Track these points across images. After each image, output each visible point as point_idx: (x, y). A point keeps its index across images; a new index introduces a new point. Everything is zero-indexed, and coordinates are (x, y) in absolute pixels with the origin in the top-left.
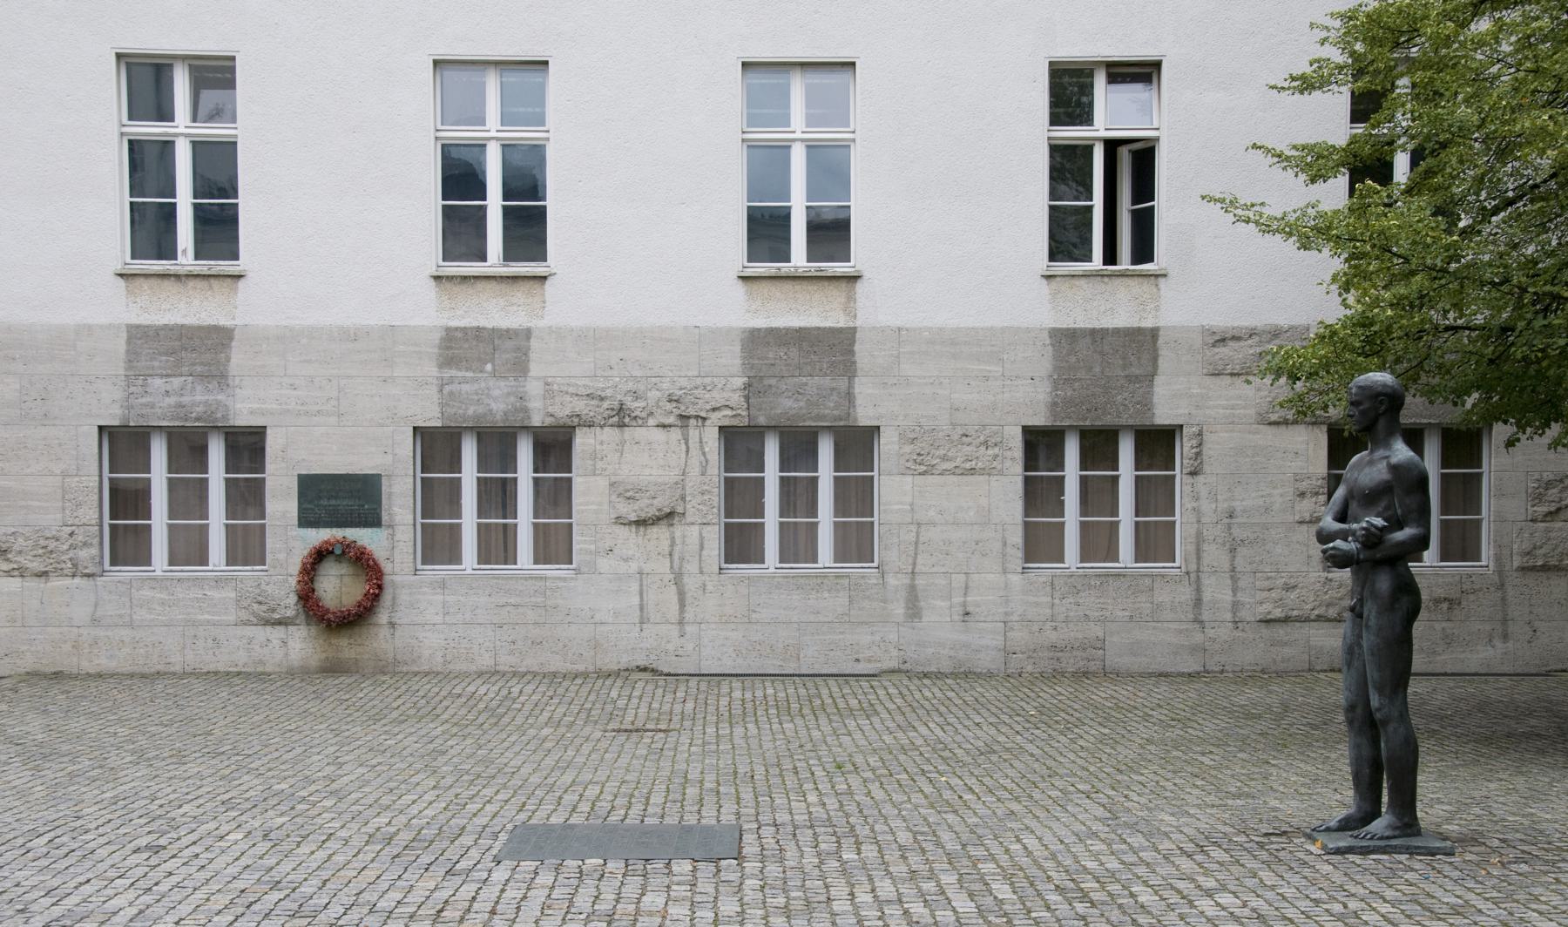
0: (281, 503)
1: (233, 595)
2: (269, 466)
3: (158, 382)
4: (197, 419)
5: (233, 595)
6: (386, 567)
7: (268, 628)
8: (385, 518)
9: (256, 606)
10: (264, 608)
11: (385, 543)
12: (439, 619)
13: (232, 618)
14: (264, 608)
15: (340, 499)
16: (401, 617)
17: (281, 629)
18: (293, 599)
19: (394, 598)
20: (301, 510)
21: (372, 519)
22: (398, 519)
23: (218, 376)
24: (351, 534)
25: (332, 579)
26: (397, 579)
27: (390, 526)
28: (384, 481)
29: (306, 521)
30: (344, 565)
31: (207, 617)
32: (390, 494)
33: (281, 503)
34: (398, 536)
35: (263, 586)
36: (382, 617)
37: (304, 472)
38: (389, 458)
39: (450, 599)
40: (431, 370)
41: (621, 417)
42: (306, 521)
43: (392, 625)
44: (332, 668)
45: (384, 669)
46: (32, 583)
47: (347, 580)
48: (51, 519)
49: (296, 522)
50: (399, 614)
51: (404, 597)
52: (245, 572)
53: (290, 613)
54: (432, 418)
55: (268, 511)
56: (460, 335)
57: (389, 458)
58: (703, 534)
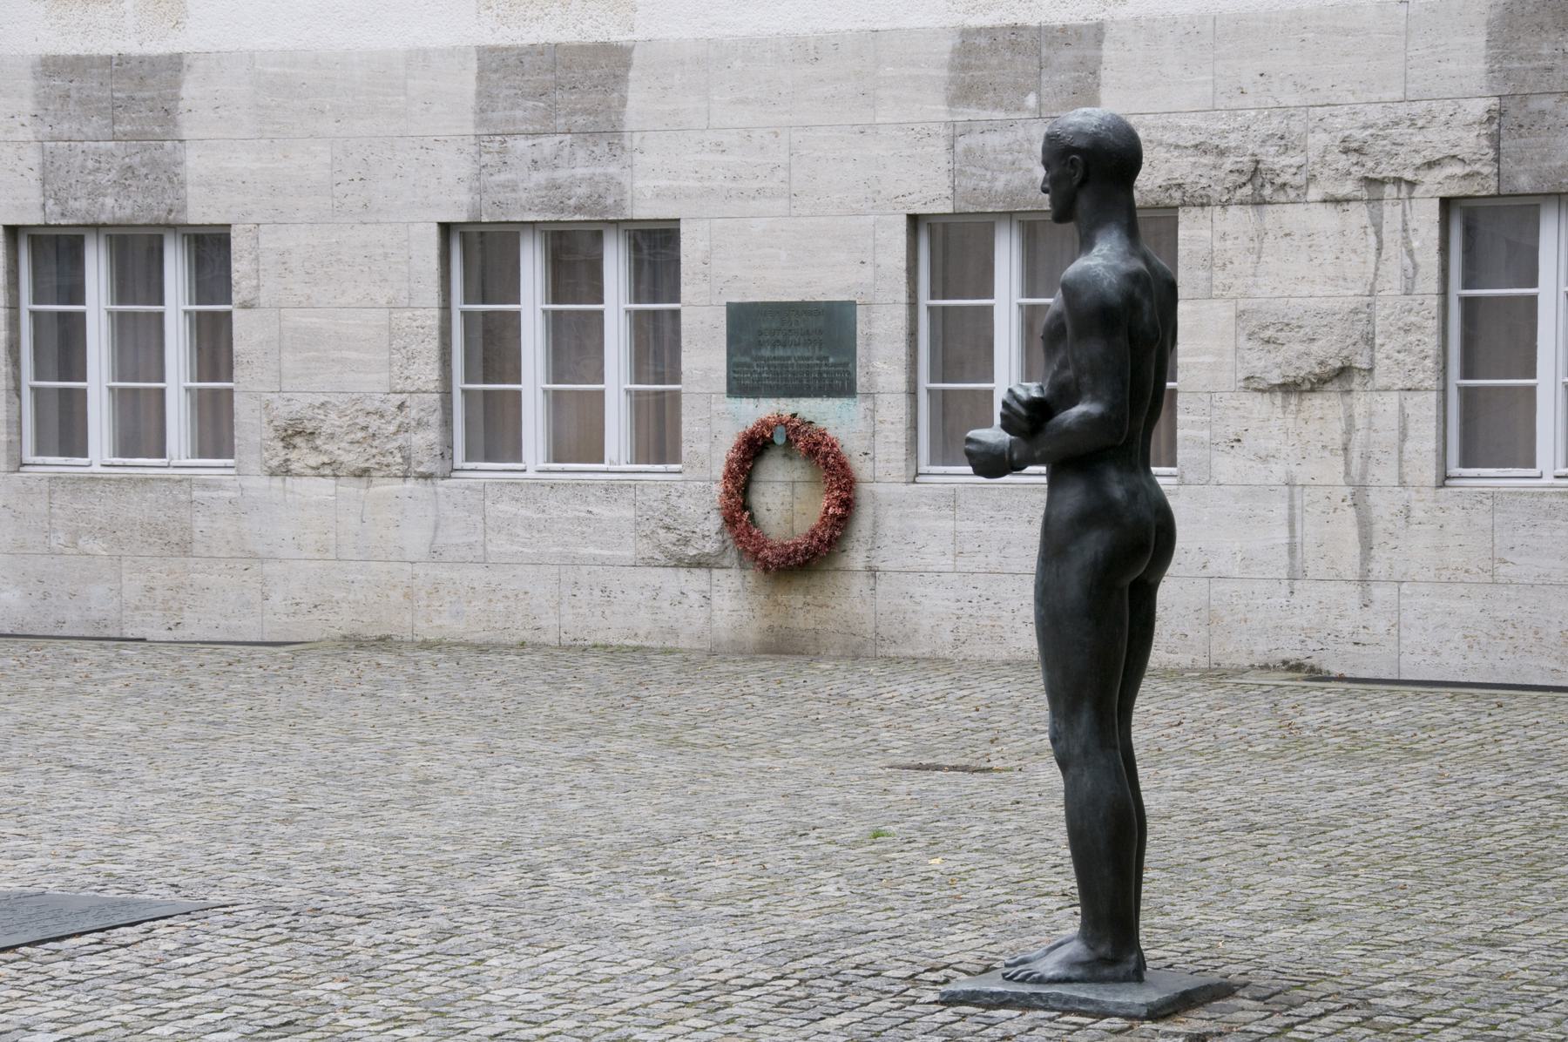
0: (704, 357)
1: (630, 513)
2: (685, 290)
3: (521, 144)
4: (579, 209)
5: (630, 513)
6: (861, 468)
7: (683, 572)
8: (861, 380)
9: (662, 532)
10: (673, 537)
11: (861, 426)
12: (945, 563)
13: (628, 553)
14: (673, 537)
15: (794, 346)
16: (890, 558)
17: (701, 574)
18: (715, 522)
19: (875, 525)
20: (733, 367)
21: (840, 384)
22: (881, 381)
23: (606, 132)
24: (810, 408)
25: (779, 488)
26: (880, 489)
27: (869, 395)
28: (860, 311)
29: (740, 386)
30: (798, 464)
31: (592, 550)
32: (869, 337)
33: (704, 357)
34: (883, 413)
35: (673, 499)
36: (856, 557)
37: (736, 299)
38: (868, 271)
39: (967, 527)
40: (936, 110)
41: (1258, 186)
42: (740, 386)
43: (872, 572)
44: (781, 646)
45: (859, 651)
46: (351, 488)
47: (800, 488)
48: (372, 383)
49: (724, 388)
50: (883, 553)
51: (891, 522)
52: (656, 474)
53: (711, 546)
54: (935, 196)
55: (684, 367)
56: (983, 41)
57: (868, 271)
58: (1406, 412)
